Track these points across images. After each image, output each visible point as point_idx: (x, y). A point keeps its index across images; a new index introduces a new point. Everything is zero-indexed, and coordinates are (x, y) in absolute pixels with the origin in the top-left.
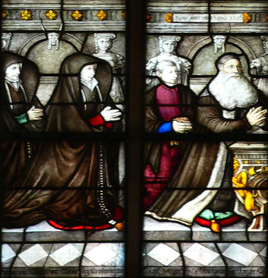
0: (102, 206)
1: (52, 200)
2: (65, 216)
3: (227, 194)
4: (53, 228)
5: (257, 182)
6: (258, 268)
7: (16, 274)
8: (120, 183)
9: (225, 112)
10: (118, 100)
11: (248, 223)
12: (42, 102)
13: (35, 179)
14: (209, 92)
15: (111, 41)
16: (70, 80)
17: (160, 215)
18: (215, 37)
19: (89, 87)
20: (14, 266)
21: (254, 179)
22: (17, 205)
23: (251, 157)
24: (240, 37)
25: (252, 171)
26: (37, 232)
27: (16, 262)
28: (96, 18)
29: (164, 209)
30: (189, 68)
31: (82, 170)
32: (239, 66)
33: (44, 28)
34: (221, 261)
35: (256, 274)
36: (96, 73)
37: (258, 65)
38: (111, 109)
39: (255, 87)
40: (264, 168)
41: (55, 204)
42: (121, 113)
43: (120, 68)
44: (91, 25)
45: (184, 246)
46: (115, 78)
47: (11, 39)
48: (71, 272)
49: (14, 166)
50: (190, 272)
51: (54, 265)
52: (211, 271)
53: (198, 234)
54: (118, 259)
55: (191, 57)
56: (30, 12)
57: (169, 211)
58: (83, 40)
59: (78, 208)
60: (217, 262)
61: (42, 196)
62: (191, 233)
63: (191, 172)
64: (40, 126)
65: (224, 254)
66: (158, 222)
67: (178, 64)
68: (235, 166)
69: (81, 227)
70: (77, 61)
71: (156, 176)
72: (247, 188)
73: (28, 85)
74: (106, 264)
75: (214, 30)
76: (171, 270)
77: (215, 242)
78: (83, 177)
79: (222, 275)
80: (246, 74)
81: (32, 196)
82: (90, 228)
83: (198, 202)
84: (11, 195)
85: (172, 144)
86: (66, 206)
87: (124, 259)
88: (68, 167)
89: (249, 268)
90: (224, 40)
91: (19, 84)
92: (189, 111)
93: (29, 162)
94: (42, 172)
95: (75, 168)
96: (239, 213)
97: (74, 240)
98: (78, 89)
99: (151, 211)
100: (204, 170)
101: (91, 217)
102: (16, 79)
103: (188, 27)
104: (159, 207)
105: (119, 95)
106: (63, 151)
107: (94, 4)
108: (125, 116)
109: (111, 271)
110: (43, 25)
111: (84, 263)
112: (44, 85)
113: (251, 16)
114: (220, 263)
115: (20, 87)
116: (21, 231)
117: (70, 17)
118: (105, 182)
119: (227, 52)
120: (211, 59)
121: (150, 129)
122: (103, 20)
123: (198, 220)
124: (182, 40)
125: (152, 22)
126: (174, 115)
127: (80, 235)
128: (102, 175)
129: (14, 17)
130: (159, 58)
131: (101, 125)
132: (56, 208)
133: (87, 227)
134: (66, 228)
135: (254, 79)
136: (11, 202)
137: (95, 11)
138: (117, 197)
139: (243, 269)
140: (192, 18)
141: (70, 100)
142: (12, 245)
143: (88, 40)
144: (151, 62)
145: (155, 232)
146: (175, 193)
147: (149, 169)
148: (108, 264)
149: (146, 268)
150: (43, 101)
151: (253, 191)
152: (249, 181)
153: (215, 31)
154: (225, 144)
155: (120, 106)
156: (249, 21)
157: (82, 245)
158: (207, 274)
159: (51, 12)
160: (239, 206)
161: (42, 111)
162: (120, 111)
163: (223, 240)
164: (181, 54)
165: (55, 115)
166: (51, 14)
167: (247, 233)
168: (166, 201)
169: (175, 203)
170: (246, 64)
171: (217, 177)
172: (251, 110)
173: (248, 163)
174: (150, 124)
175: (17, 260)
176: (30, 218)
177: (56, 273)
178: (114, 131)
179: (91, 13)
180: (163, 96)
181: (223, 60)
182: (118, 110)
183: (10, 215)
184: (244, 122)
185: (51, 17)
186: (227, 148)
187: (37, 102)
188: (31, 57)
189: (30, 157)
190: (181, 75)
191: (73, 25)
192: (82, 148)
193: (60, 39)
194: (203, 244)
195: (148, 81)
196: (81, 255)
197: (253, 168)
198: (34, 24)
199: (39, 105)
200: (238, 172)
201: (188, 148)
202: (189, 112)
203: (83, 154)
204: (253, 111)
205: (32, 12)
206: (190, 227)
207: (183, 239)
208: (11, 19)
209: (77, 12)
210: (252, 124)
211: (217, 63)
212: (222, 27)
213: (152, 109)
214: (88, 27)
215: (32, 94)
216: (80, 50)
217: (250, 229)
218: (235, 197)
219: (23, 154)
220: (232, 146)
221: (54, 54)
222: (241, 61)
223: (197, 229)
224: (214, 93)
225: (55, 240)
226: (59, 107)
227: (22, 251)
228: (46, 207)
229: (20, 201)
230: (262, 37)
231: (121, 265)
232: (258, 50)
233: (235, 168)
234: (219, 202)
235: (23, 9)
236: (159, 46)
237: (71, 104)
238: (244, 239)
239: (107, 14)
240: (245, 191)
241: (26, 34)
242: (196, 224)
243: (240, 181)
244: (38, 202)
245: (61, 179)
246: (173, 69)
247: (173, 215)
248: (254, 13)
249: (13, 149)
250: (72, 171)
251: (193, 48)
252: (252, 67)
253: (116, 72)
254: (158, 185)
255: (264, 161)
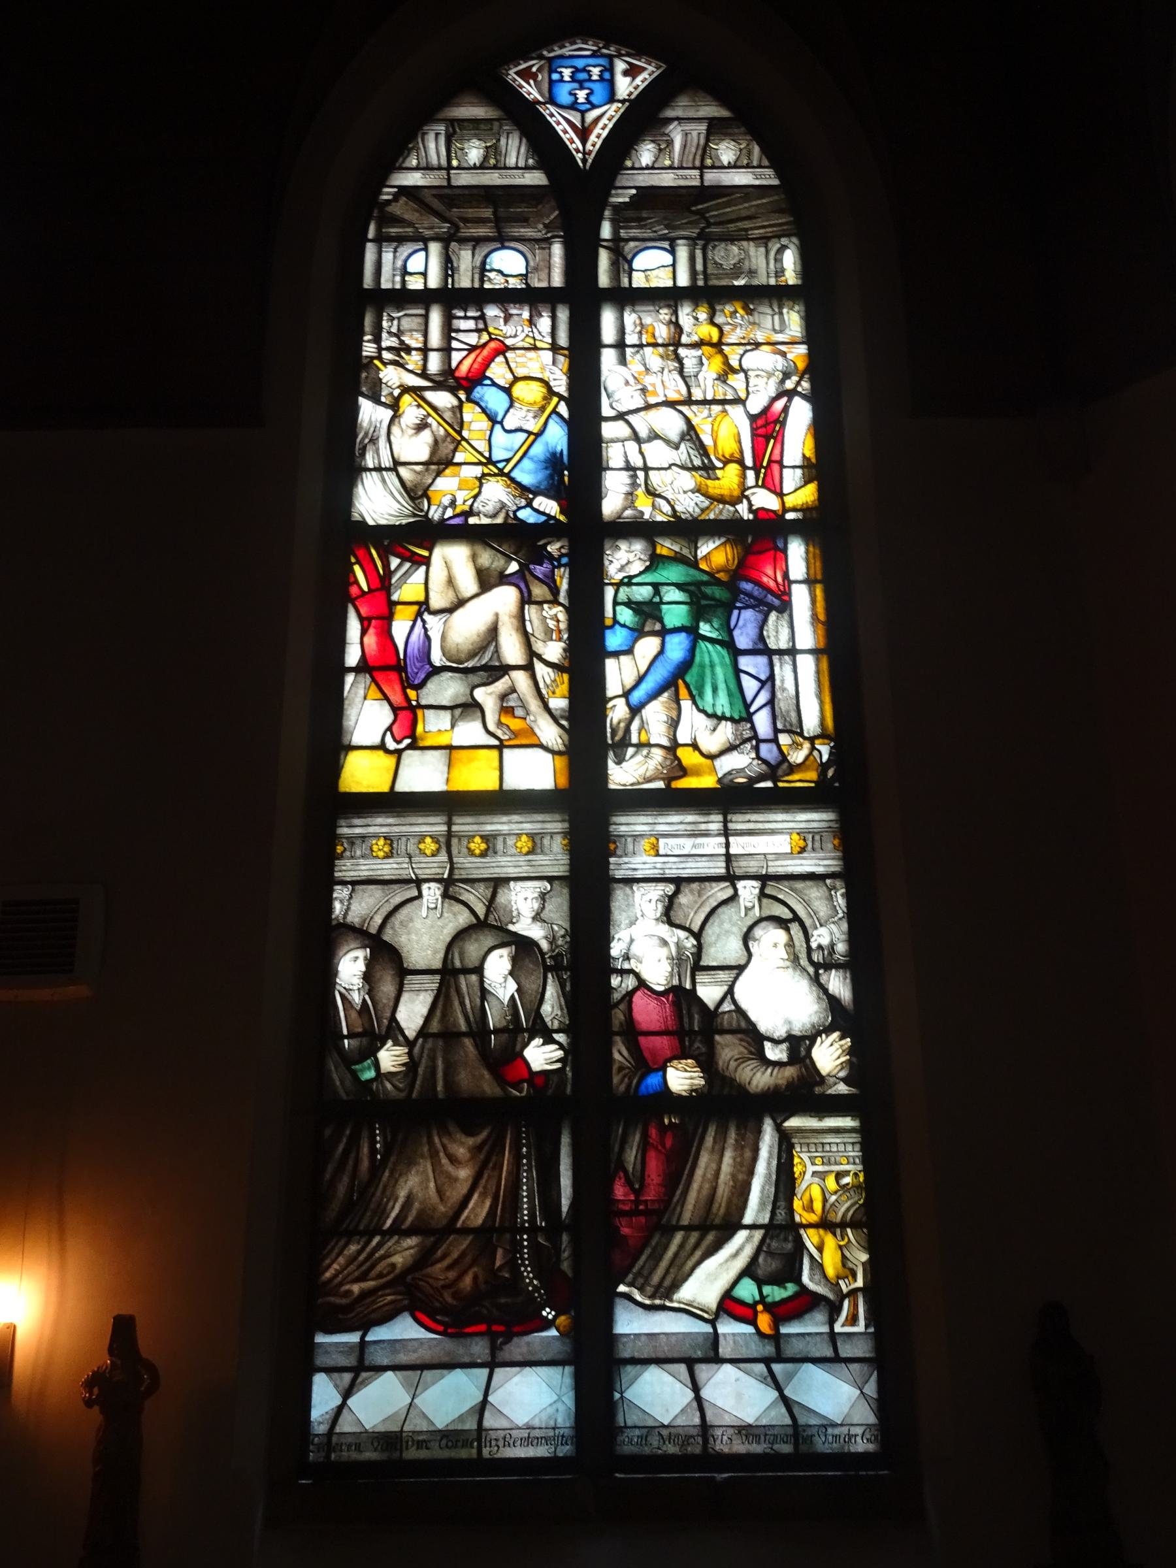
0: (527, 1272)
1: (423, 1259)
2: (450, 1300)
3: (786, 1240)
4: (423, 1330)
5: (843, 1209)
6: (864, 1427)
7: (341, 1451)
8: (564, 1215)
9: (768, 1045)
10: (556, 1025)
11: (834, 1310)
12: (407, 1033)
13: (388, 1211)
14: (734, 1002)
15: (543, 897)
16: (462, 979)
17: (649, 1294)
18: (740, 885)
19: (501, 996)
20: (337, 1430)
21: (836, 1200)
22: (349, 1275)
23: (827, 1148)
24: (786, 883)
25: (831, 1183)
26: (389, 1341)
27: (341, 1420)
28: (513, 851)
29: (656, 1279)
30: (694, 950)
31: (485, 1188)
32: (790, 944)
33: (414, 873)
34: (783, 1410)
35: (861, 1446)
36: (513, 966)
37: (825, 941)
38: (543, 1044)
39: (825, 990)
40: (856, 1175)
41: (429, 1270)
42: (562, 1052)
43: (560, 955)
44: (504, 865)
45: (702, 1370)
46: (550, 975)
47: (351, 897)
48: (460, 1444)
49: (346, 1179)
50: (718, 1442)
51: (424, 1427)
52: (762, 1438)
53: (730, 1339)
54: (562, 1408)
55: (696, 928)
56: (389, 842)
57: (667, 1283)
58: (489, 896)
59: (475, 1278)
60: (773, 1413)
61: (400, 1252)
62: (715, 1339)
63: (707, 1186)
64: (401, 1085)
65: (787, 1392)
66: (647, 1312)
67: (672, 941)
68: (797, 1170)
69: (483, 1328)
70: (476, 940)
71: (637, 1197)
72: (825, 1224)
73: (380, 994)
74: (536, 1423)
75: (736, 870)
76: (678, 1435)
77: (767, 1361)
78: (488, 1203)
79: (786, 1448)
80: (804, 962)
81: (382, 1252)
82: (501, 1328)
83: (727, 1261)
84: (336, 1251)
85: (666, 1121)
86: (452, 1275)
87: (573, 1409)
88: (456, 1180)
89: (845, 1430)
90: (757, 891)
91: (362, 993)
92: (697, 1044)
93: (376, 1169)
94: (402, 1194)
95: (469, 1183)
96: (812, 1286)
97: (467, 1360)
98: (478, 1001)
99: (630, 1285)
100: (734, 1181)
101: (503, 1301)
102: (357, 982)
103: (688, 865)
104: (645, 1273)
105: (559, 1013)
106: (445, 1141)
107: (510, 822)
108: (570, 1058)
109: (547, 1439)
110: (413, 868)
111: (488, 1422)
112: (411, 993)
113: (805, 840)
114: (780, 1416)
115: (364, 1000)
116: (353, 1338)
117: (464, 850)
118: (532, 1215)
119: (764, 916)
120: (735, 929)
121: (622, 1088)
122: (528, 853)
123: (729, 1305)
124: (677, 892)
125: (620, 857)
126: (668, 1054)
127: (479, 1348)
128: (526, 1197)
129: (358, 853)
130: (635, 931)
131: (525, 1081)
132: (430, 1280)
133: (495, 1328)
134: (449, 1331)
135: (821, 971)
136: (336, 1266)
137: (512, 837)
138: (558, 1252)
139: (830, 1431)
140: (694, 846)
141: (463, 1027)
142: (335, 1375)
143: (499, 896)
144: (619, 939)
145: (637, 1336)
146: (678, 1237)
147: (623, 1180)
148: (541, 1421)
149: (622, 1432)
150: (409, 1028)
151: (838, 1231)
152: (828, 1205)
153: (738, 872)
154: (774, 1120)
155: (560, 1037)
156: (803, 850)
157: (485, 1372)
158: (754, 1445)
159: (428, 840)
160: (811, 1269)
161: (407, 1051)
162: (561, 1047)
163: (784, 1356)
164: (678, 922)
165: (433, 1059)
166: (429, 846)
167: (833, 1336)
168: (660, 1258)
169: (678, 1262)
170: (803, 939)
171: (761, 1199)
172: (819, 1038)
173: (823, 1163)
174: (621, 1075)
175: (345, 1414)
176: (375, 1307)
177: (427, 1448)
178: (550, 1092)
179: (505, 842)
180: (647, 1012)
181: (758, 932)
182: (557, 1047)
183: (332, 1299)
184: (807, 1068)
185: (428, 852)
186: (778, 1128)
187: (397, 1032)
188: (387, 936)
189: (379, 1157)
190: (679, 966)
191: (469, 865)
192: (484, 1135)
193: (446, 895)
194: (742, 1365)
195: (615, 981)
196: (481, 1398)
197: (833, 1175)
198: (395, 866)
199: (401, 1038)
200: (804, 1185)
201: (700, 1131)
202: (698, 1048)
203: (486, 1148)
204: (822, 1042)
205: (392, 841)
206: (713, 1323)
207: (699, 1354)
208: (352, 857)
209: (478, 840)
210: (824, 1072)
211: (747, 937)
212: (752, 863)
213: (623, 1043)
214: (497, 870)
215: (388, 1015)
216: (482, 917)
217: (838, 1328)
218: (800, 1246)
219: (365, 1150)
220: (786, 1124)
221: (432, 927)
222: (792, 932)
223: (728, 1328)
224: (744, 1005)
225: (427, 1362)
226: (440, 1043)
227: (355, 1389)
228: (409, 1278)
229: (356, 1263)
230: (828, 881)
231: (568, 1425)
232: (823, 909)
233: (796, 1176)
234: (769, 1260)
235: (376, 836)
236: (633, 905)
237: (464, 1034)
238: (829, 1353)
239: (533, 841)
240: (822, 1231)
241: (379, 887)
242: (725, 1316)
243: (810, 1208)
244: (393, 1265)
245: (442, 1208)
246: (664, 952)
247: (674, 1293)
248: (809, 832)
249: (345, 1140)
250: (463, 1189)
251: (699, 907)
252: (814, 945)
253: (553, 963)
254: (643, 1219)
255: (854, 1157)
